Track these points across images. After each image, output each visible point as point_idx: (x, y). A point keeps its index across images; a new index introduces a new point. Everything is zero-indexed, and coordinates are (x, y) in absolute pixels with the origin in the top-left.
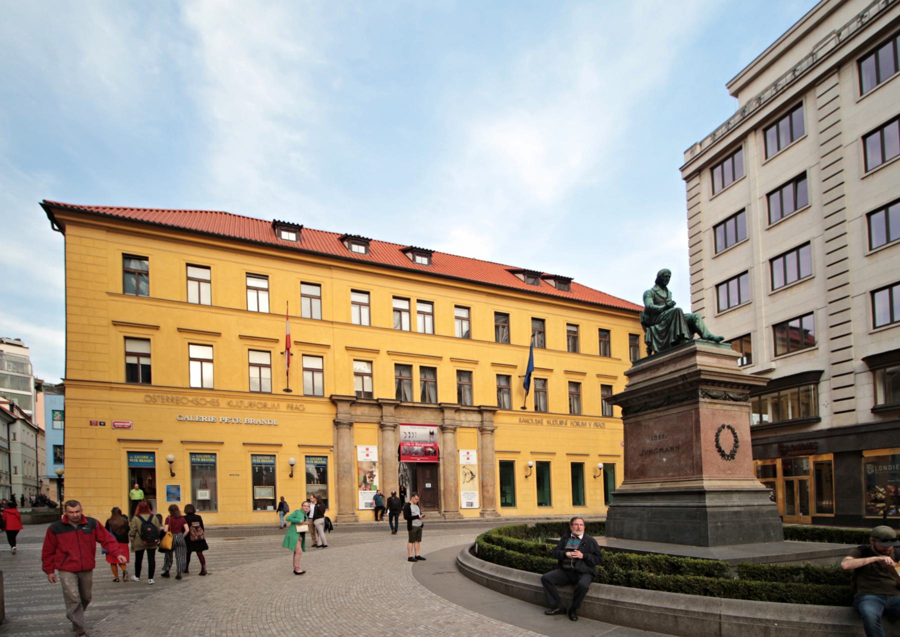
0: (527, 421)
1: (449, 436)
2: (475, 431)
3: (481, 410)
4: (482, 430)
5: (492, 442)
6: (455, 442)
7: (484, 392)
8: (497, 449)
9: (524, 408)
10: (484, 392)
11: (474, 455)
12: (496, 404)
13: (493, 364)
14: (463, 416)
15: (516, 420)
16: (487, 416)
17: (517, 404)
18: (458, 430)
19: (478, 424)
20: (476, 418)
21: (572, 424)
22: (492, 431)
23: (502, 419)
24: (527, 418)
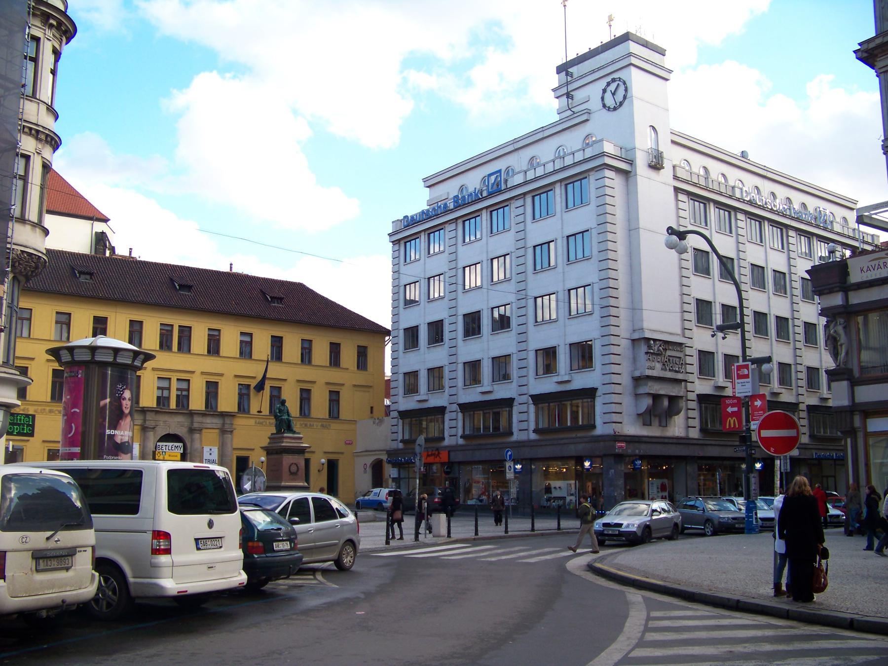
0: (261, 423)
1: (197, 436)
2: (217, 431)
3: (223, 415)
4: (223, 432)
5: (232, 440)
6: (201, 441)
7: (227, 401)
8: (235, 446)
9: (260, 412)
10: (227, 401)
11: (215, 450)
12: (236, 410)
13: (236, 376)
14: (208, 420)
15: (252, 422)
16: (228, 421)
17: (254, 409)
18: (204, 431)
19: (219, 426)
20: (217, 421)
21: (301, 425)
22: (232, 432)
23: (241, 422)
24: (262, 421)
